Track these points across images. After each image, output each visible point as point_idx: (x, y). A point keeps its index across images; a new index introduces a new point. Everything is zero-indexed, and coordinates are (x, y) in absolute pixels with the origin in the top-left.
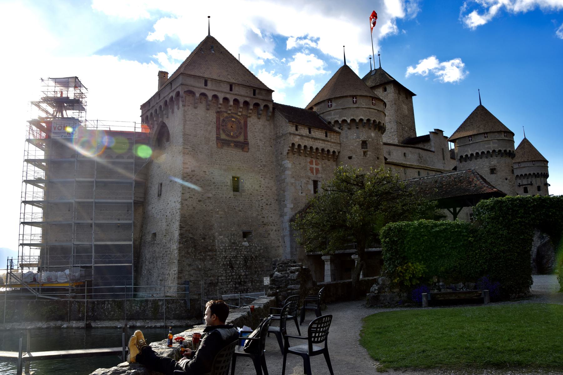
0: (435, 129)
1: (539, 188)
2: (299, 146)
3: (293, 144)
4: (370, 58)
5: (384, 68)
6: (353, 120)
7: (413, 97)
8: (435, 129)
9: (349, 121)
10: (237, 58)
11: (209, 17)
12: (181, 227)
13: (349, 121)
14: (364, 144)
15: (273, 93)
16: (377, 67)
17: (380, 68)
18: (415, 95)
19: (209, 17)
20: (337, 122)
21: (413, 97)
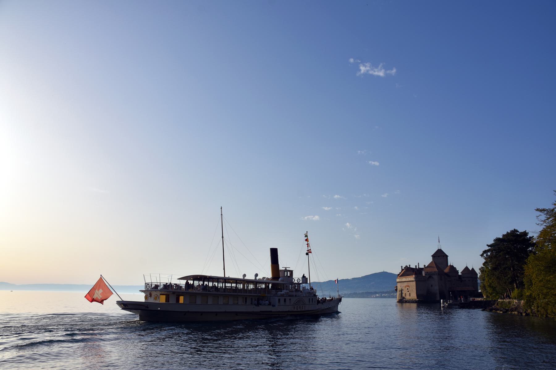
1: (475, 281)
16: (440, 249)
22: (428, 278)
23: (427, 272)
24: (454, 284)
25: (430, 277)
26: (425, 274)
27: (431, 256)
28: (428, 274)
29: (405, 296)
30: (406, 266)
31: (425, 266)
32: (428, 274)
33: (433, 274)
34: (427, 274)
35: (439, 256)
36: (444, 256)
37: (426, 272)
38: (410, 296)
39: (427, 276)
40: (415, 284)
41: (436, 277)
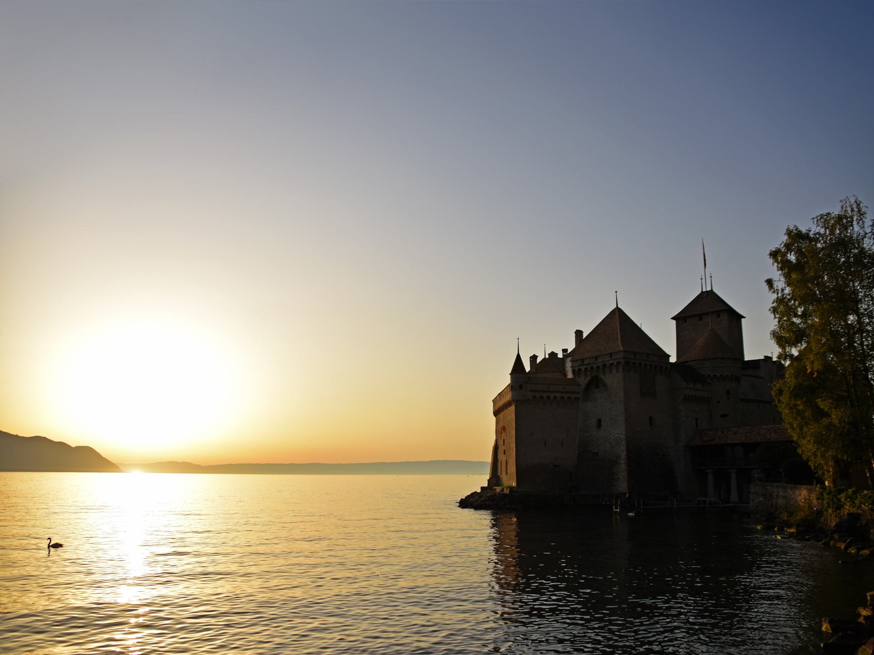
0: (765, 356)
2: (689, 396)
3: (686, 395)
4: (702, 279)
5: (715, 290)
6: (721, 376)
7: (743, 319)
8: (765, 356)
9: (718, 376)
10: (640, 326)
11: (616, 292)
12: (628, 450)
13: (718, 376)
14: (728, 392)
15: (670, 358)
16: (709, 289)
17: (712, 290)
18: (744, 317)
19: (616, 292)
20: (709, 376)
21: (743, 319)
22: (588, 387)
23: (583, 360)
24: (723, 416)
25: (595, 383)
26: (574, 372)
27: (672, 318)
28: (583, 368)
29: (501, 474)
30: (553, 355)
31: (579, 333)
32: (586, 369)
33: (605, 365)
34: (580, 370)
35: (701, 317)
36: (718, 313)
37: (576, 361)
38: (507, 474)
39: (583, 381)
40: (514, 417)
41: (614, 380)
